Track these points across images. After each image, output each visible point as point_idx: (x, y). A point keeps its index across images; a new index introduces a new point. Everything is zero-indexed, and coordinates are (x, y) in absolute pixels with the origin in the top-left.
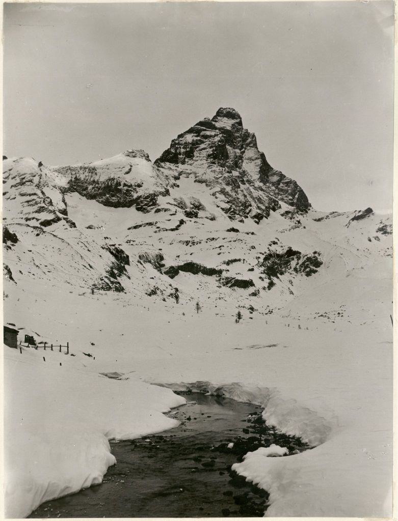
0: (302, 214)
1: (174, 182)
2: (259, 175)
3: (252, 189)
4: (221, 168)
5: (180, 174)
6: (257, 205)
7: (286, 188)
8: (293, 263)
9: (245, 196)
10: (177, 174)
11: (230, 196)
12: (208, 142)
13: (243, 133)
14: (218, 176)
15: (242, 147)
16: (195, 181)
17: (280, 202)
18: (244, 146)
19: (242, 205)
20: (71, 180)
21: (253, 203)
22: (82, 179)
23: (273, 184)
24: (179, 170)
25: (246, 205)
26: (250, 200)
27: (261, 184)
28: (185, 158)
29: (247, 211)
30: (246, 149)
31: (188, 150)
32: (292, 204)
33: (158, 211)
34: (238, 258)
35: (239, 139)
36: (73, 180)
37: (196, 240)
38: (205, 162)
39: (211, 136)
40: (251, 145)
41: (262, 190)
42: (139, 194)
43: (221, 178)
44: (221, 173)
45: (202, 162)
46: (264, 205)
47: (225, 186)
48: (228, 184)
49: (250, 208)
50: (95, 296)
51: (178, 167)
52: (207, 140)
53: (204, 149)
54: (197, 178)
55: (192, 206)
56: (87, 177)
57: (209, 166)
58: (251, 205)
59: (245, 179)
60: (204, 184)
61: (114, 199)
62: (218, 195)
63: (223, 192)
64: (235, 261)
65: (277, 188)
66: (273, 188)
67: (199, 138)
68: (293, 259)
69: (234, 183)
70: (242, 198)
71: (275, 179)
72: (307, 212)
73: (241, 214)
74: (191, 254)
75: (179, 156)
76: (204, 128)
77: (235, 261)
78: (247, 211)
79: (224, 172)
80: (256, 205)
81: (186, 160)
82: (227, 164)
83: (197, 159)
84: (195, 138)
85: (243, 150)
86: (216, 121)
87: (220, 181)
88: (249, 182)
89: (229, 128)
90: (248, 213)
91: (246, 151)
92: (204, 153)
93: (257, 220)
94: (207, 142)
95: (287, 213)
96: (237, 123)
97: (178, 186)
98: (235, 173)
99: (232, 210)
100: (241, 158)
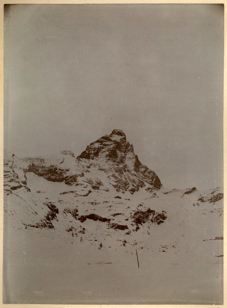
0: (157, 190)
1: (87, 169)
2: (134, 167)
3: (130, 175)
4: (113, 163)
6: (132, 184)
7: (149, 175)
8: (151, 217)
10: (89, 165)
11: (117, 178)
13: (126, 144)
14: (111, 167)
15: (125, 152)
16: (99, 169)
17: (145, 183)
19: (124, 183)
20: (30, 165)
21: (130, 183)
22: (36, 165)
23: (142, 173)
24: (90, 162)
25: (126, 184)
26: (129, 181)
27: (135, 173)
28: (94, 156)
30: (127, 153)
31: (96, 152)
32: (152, 184)
33: (77, 185)
34: (120, 213)
35: (124, 147)
36: (31, 165)
37: (97, 202)
38: (104, 159)
39: (108, 145)
40: (131, 151)
41: (135, 176)
42: (67, 175)
43: (113, 168)
47: (114, 173)
48: (117, 172)
49: (128, 185)
50: (27, 230)
53: (104, 152)
54: (100, 168)
55: (96, 183)
56: (39, 164)
57: (106, 162)
58: (129, 184)
60: (103, 171)
61: (53, 177)
62: (111, 177)
63: (114, 176)
64: (118, 214)
65: (143, 175)
66: (142, 175)
67: (102, 146)
68: (151, 215)
69: (120, 171)
70: (124, 180)
71: (143, 170)
72: (160, 189)
73: (123, 188)
74: (94, 210)
75: (91, 155)
76: (105, 140)
77: (118, 214)
80: (131, 184)
81: (94, 157)
82: (116, 161)
83: (100, 157)
84: (100, 146)
85: (126, 153)
86: (111, 137)
87: (112, 170)
89: (119, 141)
90: (127, 188)
91: (128, 154)
92: (104, 154)
93: (132, 192)
94: (106, 148)
95: (149, 189)
96: (123, 138)
97: (89, 172)
98: (121, 166)
99: (118, 186)
100: (124, 157)
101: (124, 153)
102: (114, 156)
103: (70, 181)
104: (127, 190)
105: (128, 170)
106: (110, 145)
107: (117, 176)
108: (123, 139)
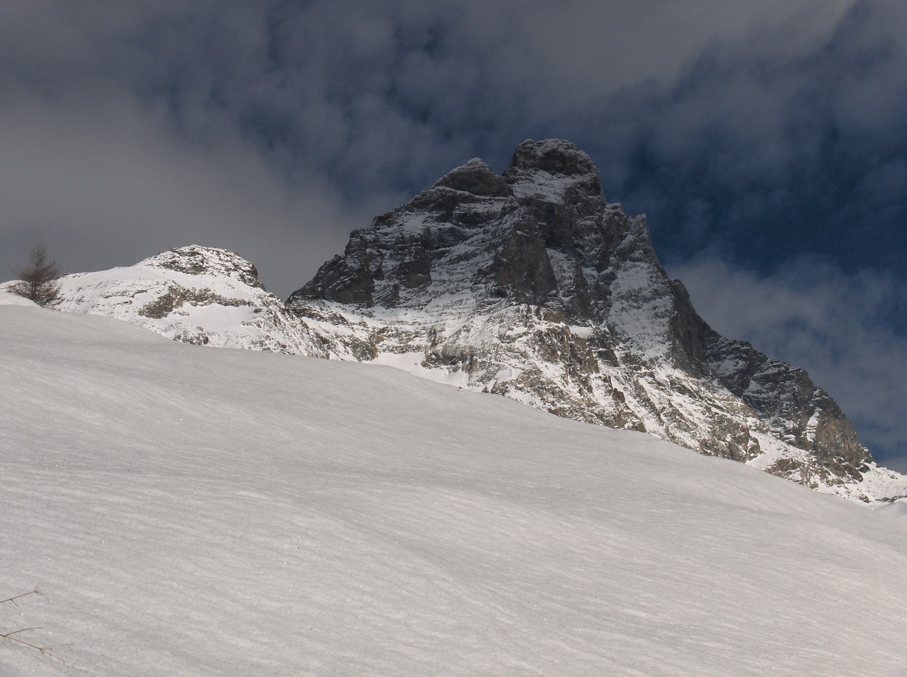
5: (379, 335)
6: (667, 430)
9: (618, 396)
10: (362, 336)
11: (561, 395)
12: (481, 236)
18: (612, 258)
26: (642, 412)
27: (679, 374)
30: (618, 267)
39: (490, 216)
40: (637, 254)
41: (683, 390)
43: (524, 338)
46: (693, 436)
47: (541, 365)
48: (550, 355)
51: (370, 315)
52: (474, 231)
54: (439, 348)
59: (618, 354)
67: (448, 225)
76: (467, 193)
79: (535, 318)
80: (661, 429)
81: (402, 294)
83: (440, 289)
84: (434, 227)
85: (610, 269)
87: (518, 345)
91: (620, 274)
94: (476, 234)
101: (599, 268)
102: (531, 276)
107: (558, 381)
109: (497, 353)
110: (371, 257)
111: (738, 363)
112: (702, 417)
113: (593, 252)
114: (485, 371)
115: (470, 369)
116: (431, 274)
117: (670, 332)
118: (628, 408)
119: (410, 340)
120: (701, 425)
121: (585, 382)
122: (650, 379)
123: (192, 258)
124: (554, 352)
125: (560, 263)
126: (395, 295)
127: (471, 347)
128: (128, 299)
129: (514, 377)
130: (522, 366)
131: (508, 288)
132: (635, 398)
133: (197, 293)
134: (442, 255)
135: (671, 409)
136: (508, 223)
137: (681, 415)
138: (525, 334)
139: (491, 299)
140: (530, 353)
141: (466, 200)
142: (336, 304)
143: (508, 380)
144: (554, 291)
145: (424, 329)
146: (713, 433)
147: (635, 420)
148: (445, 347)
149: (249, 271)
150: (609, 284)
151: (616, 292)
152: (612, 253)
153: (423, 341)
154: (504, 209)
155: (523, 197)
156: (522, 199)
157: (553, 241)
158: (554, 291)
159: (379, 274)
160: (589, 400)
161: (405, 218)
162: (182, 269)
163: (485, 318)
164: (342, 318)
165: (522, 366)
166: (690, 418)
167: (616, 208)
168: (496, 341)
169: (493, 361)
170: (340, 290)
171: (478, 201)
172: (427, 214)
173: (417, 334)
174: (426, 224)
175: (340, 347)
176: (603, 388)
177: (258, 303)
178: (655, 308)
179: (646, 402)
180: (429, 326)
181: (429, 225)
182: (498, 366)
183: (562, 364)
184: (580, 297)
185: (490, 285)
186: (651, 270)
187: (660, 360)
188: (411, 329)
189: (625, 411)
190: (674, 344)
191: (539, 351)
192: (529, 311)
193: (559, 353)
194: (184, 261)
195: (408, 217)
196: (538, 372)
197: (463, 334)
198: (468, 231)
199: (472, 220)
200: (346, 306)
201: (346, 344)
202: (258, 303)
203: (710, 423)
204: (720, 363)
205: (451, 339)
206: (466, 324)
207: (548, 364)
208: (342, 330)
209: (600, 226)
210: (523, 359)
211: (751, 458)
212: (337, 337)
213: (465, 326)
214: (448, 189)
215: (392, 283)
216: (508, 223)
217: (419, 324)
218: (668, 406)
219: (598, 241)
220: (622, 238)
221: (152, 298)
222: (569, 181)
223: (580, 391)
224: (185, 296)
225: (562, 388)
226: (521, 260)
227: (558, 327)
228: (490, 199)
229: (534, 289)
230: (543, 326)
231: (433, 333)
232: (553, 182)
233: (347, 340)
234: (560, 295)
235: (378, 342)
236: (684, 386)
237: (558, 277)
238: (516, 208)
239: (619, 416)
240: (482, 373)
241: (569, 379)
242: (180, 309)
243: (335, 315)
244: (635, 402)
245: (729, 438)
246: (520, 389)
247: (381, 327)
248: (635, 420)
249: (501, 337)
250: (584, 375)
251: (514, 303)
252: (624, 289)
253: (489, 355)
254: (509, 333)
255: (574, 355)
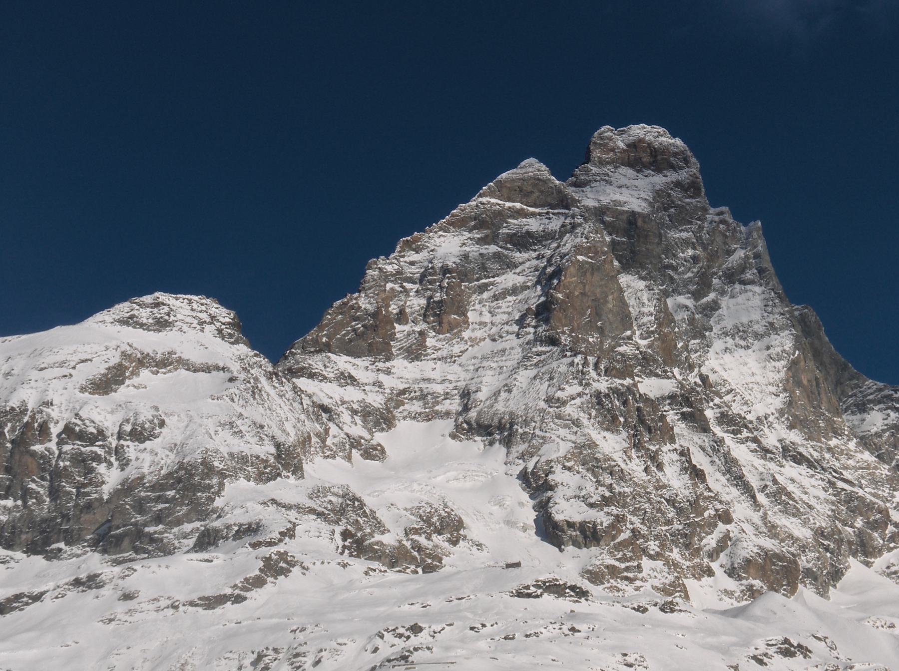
1: (358, 430)
6: (764, 517)
9: (697, 474)
10: (376, 400)
11: (622, 476)
15: (703, 285)
18: (715, 281)
21: (741, 510)
26: (731, 493)
27: (794, 436)
29: (711, 541)
30: (723, 293)
31: (437, 297)
40: (748, 275)
41: (799, 459)
43: (578, 401)
44: (581, 377)
45: (499, 345)
46: (805, 523)
48: (610, 423)
51: (388, 372)
52: (525, 255)
53: (514, 291)
54: (473, 414)
58: (726, 517)
59: (709, 414)
62: (559, 476)
67: (493, 248)
76: (518, 205)
78: (711, 541)
79: (593, 374)
80: (756, 517)
81: (430, 342)
83: (479, 334)
84: (474, 250)
85: (712, 296)
87: (569, 410)
88: (733, 423)
90: (713, 555)
91: (725, 302)
98: (651, 387)
99: (625, 535)
101: (697, 295)
102: (597, 314)
103: (158, 519)
104: (710, 573)
105: (725, 419)
106: (562, 234)
107: (618, 457)
108: (676, 194)
109: (542, 421)
110: (393, 294)
111: (888, 415)
112: (822, 494)
113: (690, 275)
114: (526, 445)
115: (508, 442)
116: (469, 314)
117: (787, 380)
118: (710, 490)
119: (438, 403)
120: (818, 507)
121: (654, 457)
122: (754, 446)
123: (155, 310)
124: (615, 419)
125: (639, 294)
126: (422, 345)
127: (511, 414)
128: (65, 371)
129: (561, 453)
130: (573, 438)
131: (564, 333)
132: (724, 474)
133: (159, 357)
134: (483, 288)
135: (775, 488)
136: (568, 246)
137: (789, 495)
138: (579, 395)
139: (540, 349)
140: (585, 422)
141: (520, 214)
142: (345, 358)
143: (554, 456)
144: (629, 333)
145: (455, 388)
146: (835, 517)
147: (719, 506)
148: (479, 413)
149: (229, 323)
150: (708, 317)
151: (719, 327)
152: (716, 274)
153: (454, 405)
154: (563, 226)
155: (596, 204)
156: (595, 208)
157: (631, 261)
158: (629, 333)
159: (402, 317)
160: (658, 481)
161: (438, 241)
162: (142, 325)
163: (532, 373)
164: (351, 377)
165: (573, 438)
166: (805, 497)
167: (721, 213)
168: (542, 405)
169: (538, 432)
170: (350, 340)
171: (533, 215)
172: (467, 235)
173: (447, 396)
174: (464, 248)
175: (346, 417)
176: (679, 464)
177: (235, 367)
178: (768, 348)
179: (739, 481)
180: (461, 384)
181: (468, 249)
182: (543, 438)
183: (624, 434)
184: (663, 338)
185: (540, 329)
186: (767, 296)
187: (771, 419)
188: (439, 389)
189: (706, 494)
190: (792, 393)
191: (596, 417)
192: (585, 363)
193: (622, 419)
194: (144, 315)
195: (442, 239)
196: (593, 445)
197: (503, 395)
198: (518, 256)
199: (523, 241)
200: (358, 361)
201: (354, 412)
202: (235, 367)
203: (833, 503)
204: (865, 415)
205: (488, 403)
206: (508, 382)
207: (607, 434)
208: (352, 394)
209: (699, 239)
210: (575, 429)
211: (890, 550)
212: (343, 403)
213: (506, 385)
214: (493, 201)
215: (418, 329)
216: (568, 246)
217: (450, 382)
218: (770, 483)
219: (695, 259)
220: (730, 253)
221: (97, 369)
222: (659, 180)
223: (646, 470)
224: (144, 361)
225: (623, 466)
226: (583, 294)
227: (622, 385)
228: (548, 213)
229: (601, 331)
230: (603, 385)
231: (466, 394)
232: (636, 182)
233: (355, 406)
234: (636, 338)
235: (397, 407)
236: (800, 454)
237: (634, 311)
238: (580, 225)
239: (696, 501)
240: (522, 447)
241: (633, 453)
242: (135, 380)
243: (342, 373)
244: (723, 480)
245: (859, 523)
246: (569, 469)
247: (402, 387)
248: (719, 506)
249: (549, 400)
250: (652, 448)
251: (569, 354)
252: (729, 324)
253: (533, 424)
254: (559, 394)
255: (641, 420)
